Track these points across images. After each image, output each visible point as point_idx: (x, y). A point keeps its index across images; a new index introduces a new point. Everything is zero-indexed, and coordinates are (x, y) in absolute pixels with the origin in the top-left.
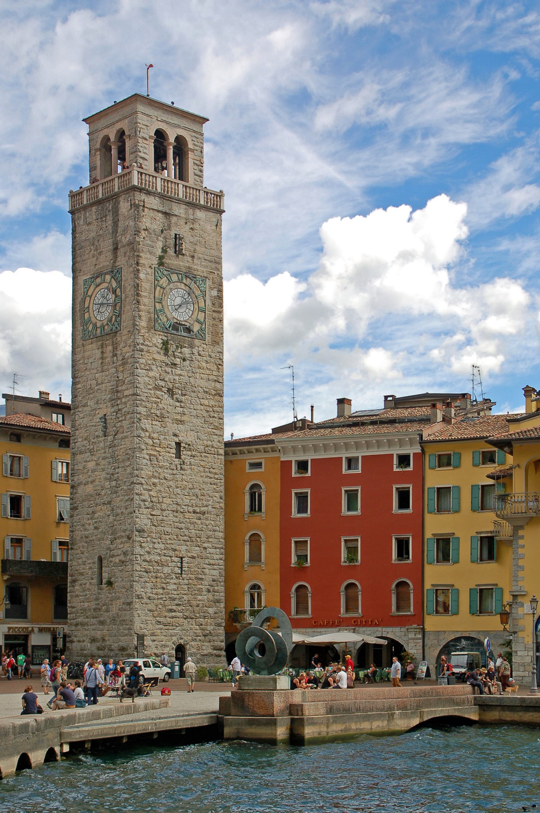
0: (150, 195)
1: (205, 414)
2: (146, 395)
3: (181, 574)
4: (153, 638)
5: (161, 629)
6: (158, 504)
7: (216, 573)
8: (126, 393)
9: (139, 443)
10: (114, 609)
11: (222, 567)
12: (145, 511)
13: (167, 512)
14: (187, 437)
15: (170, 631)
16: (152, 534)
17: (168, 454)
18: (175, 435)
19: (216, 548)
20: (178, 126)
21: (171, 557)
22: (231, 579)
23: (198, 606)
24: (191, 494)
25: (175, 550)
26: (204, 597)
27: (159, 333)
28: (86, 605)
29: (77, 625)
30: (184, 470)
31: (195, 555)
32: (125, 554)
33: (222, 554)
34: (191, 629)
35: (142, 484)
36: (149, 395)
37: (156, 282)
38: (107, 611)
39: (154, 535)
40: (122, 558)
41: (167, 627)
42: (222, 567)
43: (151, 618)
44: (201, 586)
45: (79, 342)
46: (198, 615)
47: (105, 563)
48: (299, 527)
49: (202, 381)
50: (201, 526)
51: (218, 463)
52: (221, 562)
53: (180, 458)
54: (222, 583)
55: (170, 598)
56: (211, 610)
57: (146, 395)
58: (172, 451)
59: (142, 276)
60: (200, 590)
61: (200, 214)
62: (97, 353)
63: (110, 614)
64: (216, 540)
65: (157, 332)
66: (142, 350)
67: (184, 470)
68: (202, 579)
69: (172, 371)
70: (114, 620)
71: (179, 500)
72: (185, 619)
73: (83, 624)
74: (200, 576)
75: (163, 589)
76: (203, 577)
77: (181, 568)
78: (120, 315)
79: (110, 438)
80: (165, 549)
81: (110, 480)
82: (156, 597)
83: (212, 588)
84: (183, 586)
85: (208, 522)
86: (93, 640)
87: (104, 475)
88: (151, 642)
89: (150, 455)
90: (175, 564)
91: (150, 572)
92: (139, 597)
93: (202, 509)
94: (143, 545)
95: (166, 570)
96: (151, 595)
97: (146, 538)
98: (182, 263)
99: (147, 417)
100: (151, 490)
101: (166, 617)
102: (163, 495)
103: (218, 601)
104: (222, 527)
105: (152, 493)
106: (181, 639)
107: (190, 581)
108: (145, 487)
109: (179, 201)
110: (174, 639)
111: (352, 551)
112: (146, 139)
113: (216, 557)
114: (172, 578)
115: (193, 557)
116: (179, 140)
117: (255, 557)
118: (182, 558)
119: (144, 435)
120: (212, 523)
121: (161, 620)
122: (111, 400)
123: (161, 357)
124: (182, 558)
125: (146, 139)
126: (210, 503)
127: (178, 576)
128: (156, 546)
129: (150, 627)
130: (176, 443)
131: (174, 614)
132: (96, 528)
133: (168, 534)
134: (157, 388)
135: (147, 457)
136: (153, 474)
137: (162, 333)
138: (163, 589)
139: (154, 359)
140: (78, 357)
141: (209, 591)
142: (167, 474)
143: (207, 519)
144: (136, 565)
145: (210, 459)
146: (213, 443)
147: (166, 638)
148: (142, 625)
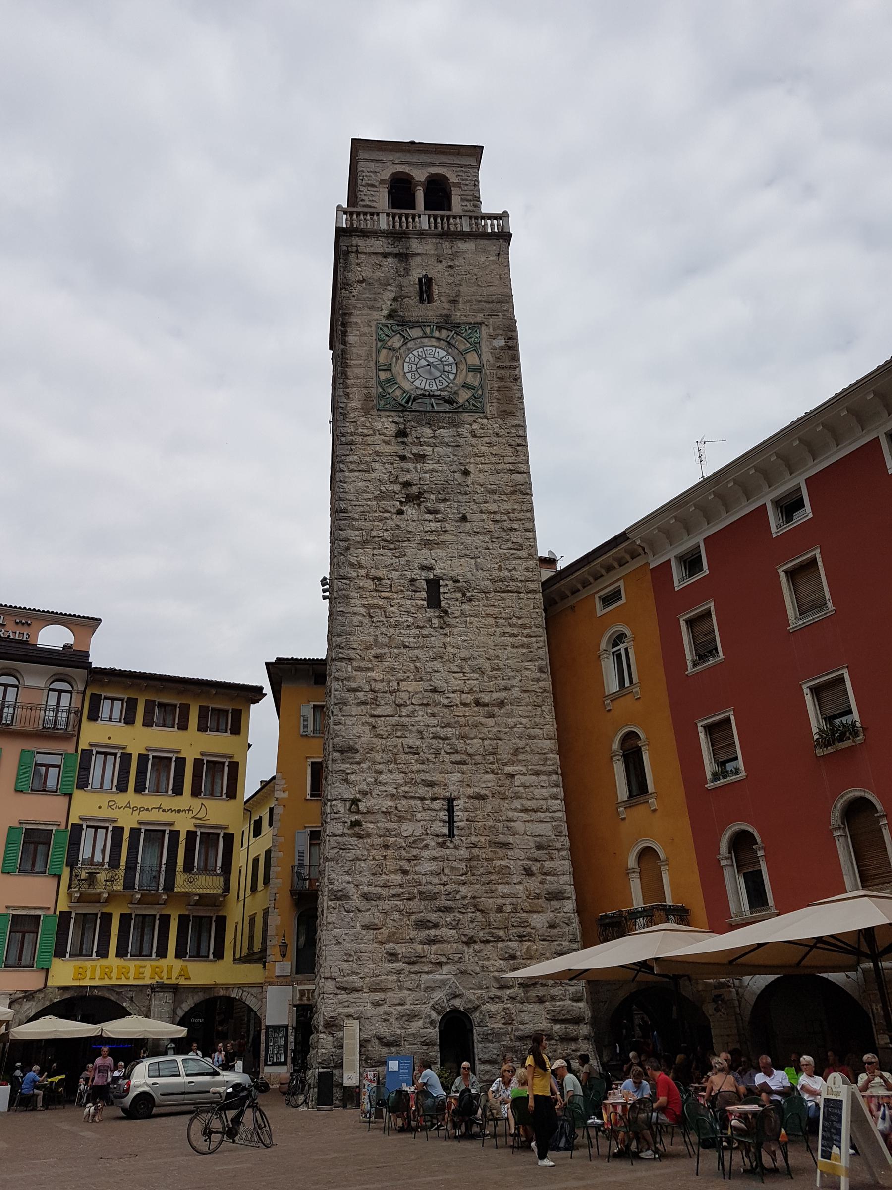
0: (367, 236)
1: (492, 527)
2: (362, 509)
3: (451, 835)
4: (377, 996)
5: (400, 972)
6: (388, 695)
7: (540, 829)
9: (344, 589)
11: (559, 814)
12: (355, 710)
13: (410, 708)
15: (424, 976)
16: (373, 754)
17: (409, 602)
18: (429, 568)
19: (537, 773)
20: (432, 164)
21: (422, 799)
23: (500, 910)
24: (467, 670)
25: (431, 785)
26: (521, 888)
27: (387, 413)
30: (449, 625)
31: (483, 792)
33: (557, 786)
34: (484, 969)
35: (350, 660)
36: (367, 509)
37: (380, 344)
39: (378, 757)
41: (415, 968)
42: (559, 814)
43: (371, 946)
44: (503, 863)
46: (501, 933)
49: (481, 475)
50: (494, 730)
51: (531, 609)
52: (557, 804)
53: (438, 606)
54: (564, 853)
55: (421, 893)
57: (362, 509)
58: (418, 595)
59: (351, 339)
60: (504, 871)
64: (537, 757)
65: (382, 413)
66: (352, 443)
67: (449, 625)
68: (505, 845)
69: (416, 467)
71: (437, 683)
72: (467, 943)
74: (501, 838)
75: (405, 872)
76: (511, 839)
77: (451, 821)
80: (406, 783)
82: (384, 892)
83: (538, 864)
84: (455, 864)
85: (511, 721)
88: (369, 1006)
89: (369, 607)
90: (433, 813)
91: (369, 836)
92: (340, 896)
93: (495, 695)
94: (352, 778)
95: (408, 828)
96: (372, 889)
97: (359, 763)
98: (431, 312)
100: (372, 669)
101: (412, 940)
102: (400, 675)
103: (556, 896)
104: (551, 729)
105: (372, 674)
106: (456, 996)
107: (475, 851)
108: (355, 664)
110: (437, 995)
112: (373, 186)
113: (538, 792)
114: (426, 847)
115: (480, 797)
117: (638, 786)
118: (451, 801)
119: (355, 574)
120: (524, 721)
121: (401, 949)
124: (451, 801)
125: (373, 186)
126: (515, 682)
127: (440, 840)
128: (382, 778)
129: (368, 968)
130: (428, 581)
131: (433, 932)
135: (363, 611)
136: (376, 640)
137: (393, 414)
138: (405, 872)
139: (378, 453)
141: (529, 872)
142: (408, 637)
143: (509, 715)
144: (333, 822)
145: (508, 603)
146: (514, 572)
147: (414, 995)
148: (345, 965)
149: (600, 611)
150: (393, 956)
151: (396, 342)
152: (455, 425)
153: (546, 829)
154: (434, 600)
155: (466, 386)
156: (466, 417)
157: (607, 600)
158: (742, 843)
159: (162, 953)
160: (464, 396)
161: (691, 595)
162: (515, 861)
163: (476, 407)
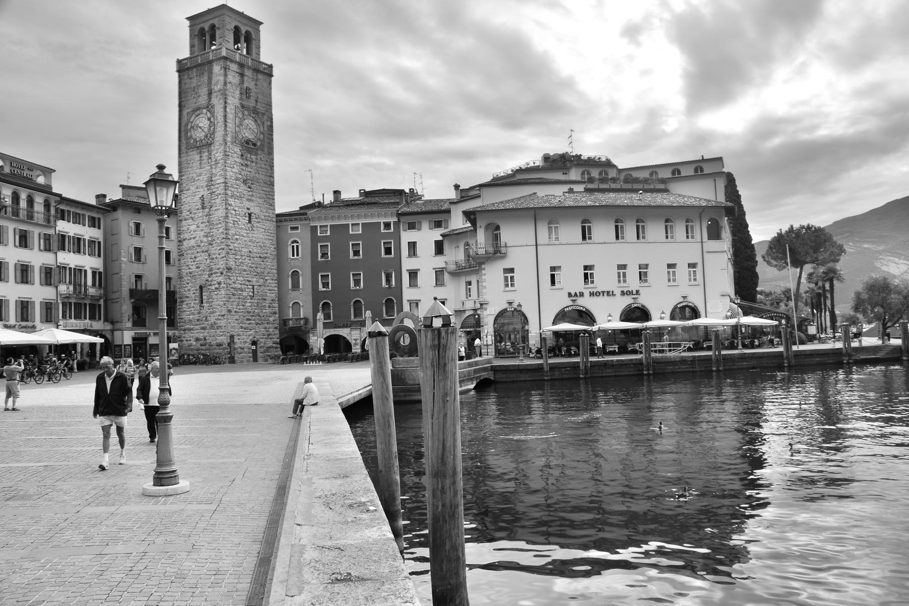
7: (273, 295)
8: (218, 182)
10: (212, 319)
12: (231, 256)
14: (255, 210)
18: (248, 209)
22: (281, 299)
26: (268, 311)
28: (191, 317)
29: (185, 330)
32: (219, 283)
38: (206, 320)
40: (217, 286)
45: (184, 150)
47: (204, 289)
48: (325, 266)
56: (271, 319)
61: (260, 76)
62: (197, 157)
63: (209, 323)
70: (212, 327)
73: (190, 330)
78: (213, 133)
79: (207, 210)
81: (207, 236)
86: (197, 340)
87: (202, 233)
92: (229, 311)
95: (245, 294)
99: (231, 197)
103: (275, 313)
109: (249, 68)
111: (357, 282)
116: (247, 32)
122: (207, 186)
123: (239, 160)
132: (198, 267)
133: (245, 271)
134: (237, 179)
140: (183, 159)
142: (244, 233)
149: (290, 231)
150: (242, 327)
151: (240, 115)
152: (256, 154)
153: (273, 295)
154: (250, 221)
155: (259, 139)
156: (259, 152)
157: (293, 228)
158: (326, 305)
159: (85, 318)
160: (259, 144)
161: (325, 239)
162: (267, 304)
163: (262, 148)
